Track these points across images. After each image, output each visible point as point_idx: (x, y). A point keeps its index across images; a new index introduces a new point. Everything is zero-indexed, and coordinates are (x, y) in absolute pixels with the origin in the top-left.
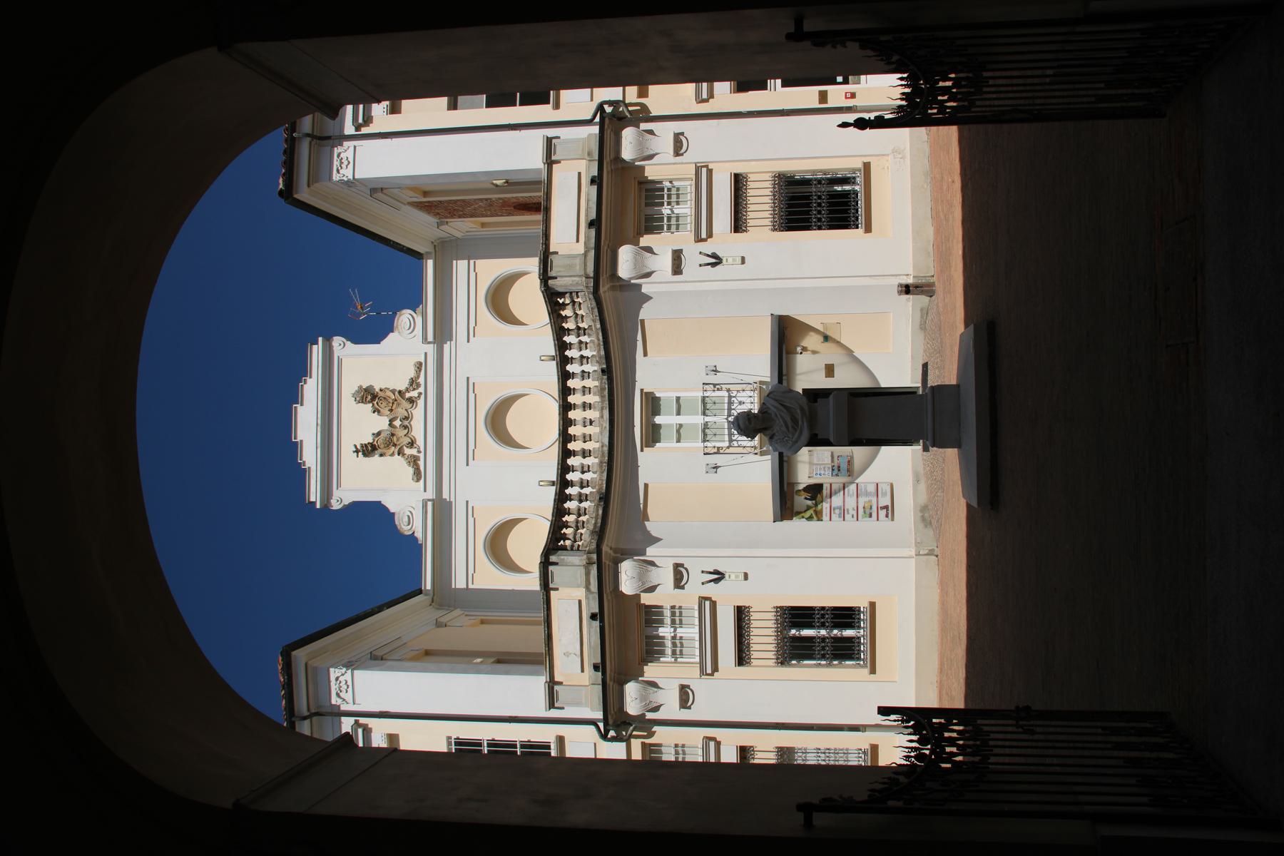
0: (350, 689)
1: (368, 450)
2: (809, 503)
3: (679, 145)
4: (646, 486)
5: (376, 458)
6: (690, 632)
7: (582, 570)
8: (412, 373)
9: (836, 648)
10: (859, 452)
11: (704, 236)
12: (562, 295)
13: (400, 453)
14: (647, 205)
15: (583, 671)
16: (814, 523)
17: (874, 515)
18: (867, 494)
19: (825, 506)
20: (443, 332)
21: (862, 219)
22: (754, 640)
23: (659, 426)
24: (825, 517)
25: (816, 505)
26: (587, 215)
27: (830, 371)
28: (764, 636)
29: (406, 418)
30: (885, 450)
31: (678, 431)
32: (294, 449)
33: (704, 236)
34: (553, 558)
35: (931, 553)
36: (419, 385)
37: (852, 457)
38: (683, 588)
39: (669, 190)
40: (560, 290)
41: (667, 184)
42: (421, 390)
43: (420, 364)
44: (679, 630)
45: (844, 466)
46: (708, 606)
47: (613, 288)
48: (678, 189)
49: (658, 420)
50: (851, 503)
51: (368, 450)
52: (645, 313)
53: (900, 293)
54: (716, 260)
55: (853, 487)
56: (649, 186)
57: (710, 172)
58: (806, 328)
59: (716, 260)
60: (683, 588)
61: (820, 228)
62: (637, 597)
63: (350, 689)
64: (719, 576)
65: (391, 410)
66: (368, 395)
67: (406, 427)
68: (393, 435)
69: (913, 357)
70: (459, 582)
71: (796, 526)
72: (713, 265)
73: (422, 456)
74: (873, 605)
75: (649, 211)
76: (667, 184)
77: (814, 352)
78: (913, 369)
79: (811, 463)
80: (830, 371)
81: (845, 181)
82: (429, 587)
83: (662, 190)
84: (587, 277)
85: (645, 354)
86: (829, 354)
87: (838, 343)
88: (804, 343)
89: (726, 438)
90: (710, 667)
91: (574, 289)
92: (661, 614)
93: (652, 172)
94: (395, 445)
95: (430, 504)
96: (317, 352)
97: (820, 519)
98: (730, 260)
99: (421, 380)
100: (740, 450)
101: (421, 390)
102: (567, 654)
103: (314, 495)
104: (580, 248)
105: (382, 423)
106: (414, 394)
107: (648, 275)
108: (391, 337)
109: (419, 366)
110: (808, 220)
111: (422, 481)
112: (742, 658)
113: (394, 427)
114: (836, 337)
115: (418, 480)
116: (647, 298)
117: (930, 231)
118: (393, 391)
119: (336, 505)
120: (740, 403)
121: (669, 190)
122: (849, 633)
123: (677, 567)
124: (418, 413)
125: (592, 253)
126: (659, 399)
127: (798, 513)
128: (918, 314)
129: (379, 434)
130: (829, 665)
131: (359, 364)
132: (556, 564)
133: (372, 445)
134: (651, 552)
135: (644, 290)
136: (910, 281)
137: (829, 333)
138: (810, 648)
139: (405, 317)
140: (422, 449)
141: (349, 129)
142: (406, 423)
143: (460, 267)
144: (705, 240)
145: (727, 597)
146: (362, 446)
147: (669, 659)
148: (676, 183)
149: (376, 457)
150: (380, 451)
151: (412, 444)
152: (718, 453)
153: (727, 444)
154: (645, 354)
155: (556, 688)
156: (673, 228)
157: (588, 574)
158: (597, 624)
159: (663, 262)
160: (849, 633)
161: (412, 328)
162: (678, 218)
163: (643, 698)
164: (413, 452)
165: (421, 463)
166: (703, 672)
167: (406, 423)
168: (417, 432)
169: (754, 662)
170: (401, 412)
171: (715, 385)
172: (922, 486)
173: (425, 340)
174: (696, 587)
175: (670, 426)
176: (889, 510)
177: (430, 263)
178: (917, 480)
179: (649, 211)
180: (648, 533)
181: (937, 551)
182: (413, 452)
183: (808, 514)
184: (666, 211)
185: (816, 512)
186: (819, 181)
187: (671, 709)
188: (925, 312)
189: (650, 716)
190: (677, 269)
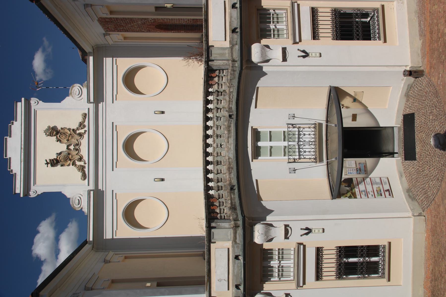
1: (54, 163)
2: (348, 188)
4: (257, 181)
6: (289, 263)
7: (231, 232)
8: (80, 119)
10: (369, 161)
11: (297, 40)
12: (214, 71)
13: (74, 164)
14: (261, 22)
15: (228, 289)
16: (353, 200)
17: (383, 194)
18: (377, 183)
19: (357, 190)
20: (99, 97)
22: (325, 265)
24: (358, 196)
25: (352, 190)
26: (230, 25)
28: (330, 263)
29: (77, 145)
30: (382, 159)
32: (6, 162)
33: (298, 40)
34: (213, 225)
35: (420, 215)
36: (84, 126)
38: (288, 238)
39: (273, 15)
40: (215, 68)
41: (272, 11)
42: (86, 129)
43: (86, 114)
44: (282, 262)
45: (363, 168)
48: (277, 15)
49: (260, 144)
50: (369, 188)
51: (54, 163)
52: (262, 83)
54: (306, 55)
55: (368, 180)
58: (346, 94)
59: (306, 55)
60: (288, 238)
61: (358, 39)
62: (262, 245)
64: (309, 231)
65: (68, 140)
66: (53, 131)
67: (77, 150)
68: (69, 154)
69: (398, 111)
70: (108, 235)
71: (344, 201)
72: (304, 57)
73: (86, 166)
74: (390, 243)
75: (263, 26)
77: (347, 107)
78: (397, 117)
80: (354, 117)
81: (366, 15)
82: (91, 239)
83: (270, 14)
84: (234, 61)
85: (256, 107)
86: (355, 109)
87: (360, 103)
89: (297, 154)
90: (301, 282)
91: (223, 68)
92: (272, 253)
94: (70, 160)
95: (92, 192)
96: (20, 107)
97: (355, 197)
98: (314, 55)
99: (86, 123)
100: (308, 160)
101: (86, 129)
102: (220, 280)
103: (19, 188)
104: (227, 44)
105: (62, 147)
106: (82, 131)
107: (268, 61)
108: (68, 100)
109: (85, 116)
110: (352, 35)
111: (87, 180)
112: (318, 277)
113: (70, 150)
115: (85, 179)
116: (265, 74)
118: (69, 129)
119: (32, 195)
120: (304, 135)
123: (286, 226)
124: (84, 142)
125: (237, 47)
126: (260, 132)
127: (343, 194)
128: (406, 88)
129: (60, 153)
130: (365, 278)
132: (214, 228)
133: (56, 160)
134: (269, 218)
135: (264, 70)
136: (408, 69)
137: (357, 97)
139: (76, 88)
140: (87, 162)
142: (77, 147)
143: (108, 62)
144: (297, 43)
145: (312, 243)
146: (50, 160)
147: (277, 279)
148: (277, 11)
149: (59, 166)
150: (61, 163)
151: (81, 159)
152: (294, 162)
153: (297, 157)
154: (256, 107)
156: (276, 36)
157: (235, 233)
159: (276, 54)
162: (278, 31)
164: (82, 163)
165: (86, 170)
166: (298, 286)
167: (77, 147)
168: (84, 152)
169: (324, 278)
170: (74, 141)
171: (292, 125)
172: (404, 178)
173: (89, 101)
175: (266, 147)
176: (390, 191)
177: (91, 58)
178: (401, 176)
179: (263, 26)
180: (264, 208)
181: (424, 214)
182: (82, 163)
183: (349, 194)
184: (272, 26)
185: (352, 193)
186: (357, 14)
188: (410, 87)
190: (285, 59)
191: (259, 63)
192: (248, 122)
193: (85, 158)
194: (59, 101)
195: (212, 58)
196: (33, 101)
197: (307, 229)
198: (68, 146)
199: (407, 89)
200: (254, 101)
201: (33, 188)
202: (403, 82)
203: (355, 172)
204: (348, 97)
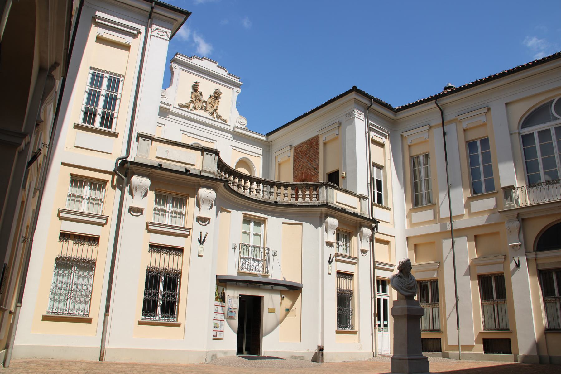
0: (159, 36)
1: (195, 88)
3: (364, 252)
5: (191, 90)
8: (223, 117)
9: (168, 303)
10: (235, 322)
11: (337, 258)
13: (192, 102)
15: (157, 157)
20: (237, 136)
21: (341, 329)
22: (163, 256)
27: (272, 311)
28: (165, 262)
29: (206, 109)
30: (236, 336)
31: (246, 233)
37: (234, 319)
38: (197, 221)
46: (185, 233)
47: (321, 214)
49: (252, 224)
51: (195, 88)
53: (319, 346)
54: (330, 262)
55: (223, 318)
57: (354, 264)
59: (330, 262)
63: (159, 36)
66: (217, 96)
67: (202, 107)
73: (189, 111)
74: (179, 325)
76: (348, 245)
77: (281, 303)
79: (234, 297)
80: (272, 311)
85: (284, 223)
86: (280, 311)
87: (285, 316)
90: (150, 228)
93: (355, 239)
99: (220, 120)
101: (216, 119)
102: (167, 151)
105: (205, 97)
107: (327, 231)
108: (238, 114)
109: (225, 121)
111: (178, 107)
112: (154, 247)
114: (288, 315)
115: (179, 105)
117: (338, 361)
118: (217, 107)
121: (346, 245)
122: (159, 310)
124: (207, 115)
126: (260, 226)
127: (217, 288)
128: (300, 355)
129: (201, 95)
131: (229, 97)
137: (291, 312)
138: (169, 288)
139: (245, 122)
141: (370, 122)
142: (204, 108)
145: (189, 244)
149: (192, 91)
150: (194, 93)
154: (284, 223)
155: (150, 141)
157: (210, 173)
158: (184, 171)
160: (159, 310)
161: (241, 123)
163: (140, 187)
164: (191, 108)
165: (186, 109)
167: (204, 108)
168: (199, 112)
170: (209, 107)
171: (268, 253)
174: (197, 229)
176: (215, 338)
177: (264, 138)
182: (191, 108)
187: (129, 202)
189: (127, 189)
191: (327, 223)
193: (194, 112)
194: (237, 107)
198: (206, 102)
199: (299, 357)
202: (306, 351)
203: (230, 306)
204: (291, 303)
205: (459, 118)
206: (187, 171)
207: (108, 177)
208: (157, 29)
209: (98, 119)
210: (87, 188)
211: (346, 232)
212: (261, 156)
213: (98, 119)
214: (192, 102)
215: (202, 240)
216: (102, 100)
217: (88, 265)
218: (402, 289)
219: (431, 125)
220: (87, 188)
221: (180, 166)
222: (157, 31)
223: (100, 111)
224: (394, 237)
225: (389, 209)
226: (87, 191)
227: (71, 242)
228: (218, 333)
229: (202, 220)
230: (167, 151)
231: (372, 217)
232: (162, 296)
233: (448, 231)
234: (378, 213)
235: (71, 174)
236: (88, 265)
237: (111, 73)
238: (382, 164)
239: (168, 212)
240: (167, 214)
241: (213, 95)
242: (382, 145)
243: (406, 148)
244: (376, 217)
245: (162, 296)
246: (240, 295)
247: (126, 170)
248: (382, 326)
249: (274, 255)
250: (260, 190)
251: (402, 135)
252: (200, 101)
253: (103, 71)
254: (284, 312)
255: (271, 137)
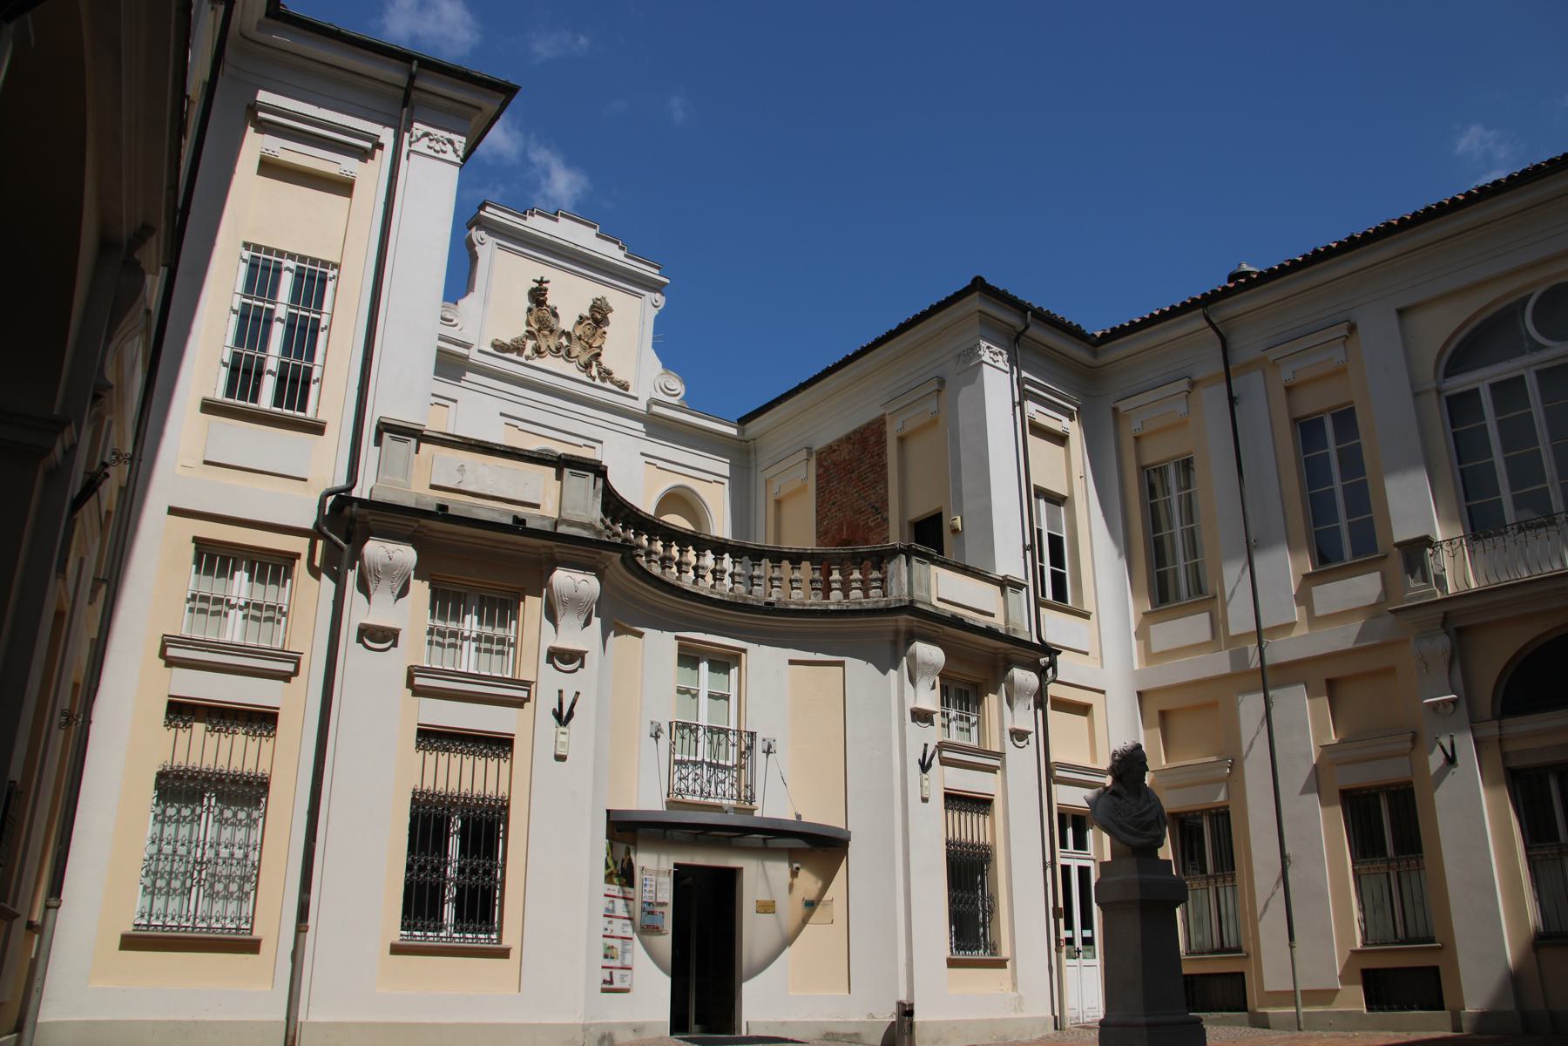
0: (432, 152)
1: (538, 295)
3: (1019, 735)
8: (617, 376)
9: (473, 892)
10: (665, 943)
11: (946, 754)
13: (530, 335)
15: (433, 487)
20: (658, 426)
21: (961, 956)
22: (456, 760)
23: (695, 667)
27: (767, 907)
28: (463, 776)
29: (569, 353)
38: (550, 660)
42: (598, 382)
46: (515, 695)
47: (897, 632)
49: (704, 666)
51: (538, 295)
52: (859, 669)
53: (900, 1004)
54: (925, 767)
55: (629, 932)
56: (972, 698)
57: (993, 769)
59: (925, 767)
63: (432, 152)
65: (579, 338)
66: (598, 316)
67: (558, 350)
69: (784, 1023)
73: (522, 359)
74: (504, 953)
76: (973, 719)
77: (791, 886)
78: (767, 1025)
79: (658, 872)
80: (767, 907)
85: (792, 662)
86: (789, 909)
87: (805, 921)
88: (804, 874)
90: (418, 684)
93: (992, 701)
99: (608, 385)
101: (598, 382)
102: (461, 469)
105: (567, 322)
106: (594, 372)
107: (912, 680)
108: (657, 365)
109: (624, 386)
111: (491, 350)
112: (430, 737)
115: (494, 346)
118: (600, 347)
121: (968, 720)
122: (449, 912)
124: (571, 369)
127: (611, 847)
128: (851, 1030)
129: (555, 315)
131: (633, 319)
133: (544, 302)
139: (678, 386)
141: (1024, 374)
142: (563, 352)
145: (527, 726)
149: (528, 304)
151: (538, 351)
154: (792, 662)
155: (414, 441)
157: (582, 525)
158: (509, 521)
160: (449, 912)
163: (388, 570)
164: (528, 351)
165: (513, 356)
167: (563, 352)
168: (550, 362)
171: (750, 748)
176: (609, 987)
177: (733, 431)
189: (352, 576)
191: (913, 657)
192: (760, 643)
193: (537, 362)
194: (655, 346)
195: (914, 559)
196: (660, 299)
197: (571, 714)
198: (568, 335)
199: (845, 1035)
200: (810, 656)
201: (491, 241)
202: (864, 1019)
203: (648, 897)
204: (820, 884)
205: (1272, 355)
206: (519, 521)
207: (300, 545)
208: (426, 135)
209: (269, 385)
210: (242, 576)
211: (967, 683)
212: (726, 481)
213: (269, 385)
214: (530, 335)
215: (565, 713)
216: (278, 332)
217: (248, 792)
218: (1121, 827)
219: (1197, 376)
220: (242, 576)
221: (498, 510)
222: (425, 140)
223: (272, 364)
224: (1103, 692)
225: (1086, 616)
226: (240, 586)
227: (199, 727)
228: (617, 973)
229: (561, 657)
230: (461, 469)
231: (1039, 638)
232: (455, 874)
233: (1254, 671)
234: (1056, 627)
235: (196, 540)
236: (248, 792)
237: (303, 259)
238: (1060, 488)
239: (467, 638)
240: (466, 644)
241: (587, 313)
242: (1061, 439)
243: (1128, 444)
244: (1050, 637)
245: (455, 874)
246: (676, 865)
247: (347, 523)
248: (1078, 943)
249: (768, 752)
250: (723, 572)
251: (1115, 410)
252: (552, 331)
253: (281, 254)
254: (800, 910)
255: (754, 427)
